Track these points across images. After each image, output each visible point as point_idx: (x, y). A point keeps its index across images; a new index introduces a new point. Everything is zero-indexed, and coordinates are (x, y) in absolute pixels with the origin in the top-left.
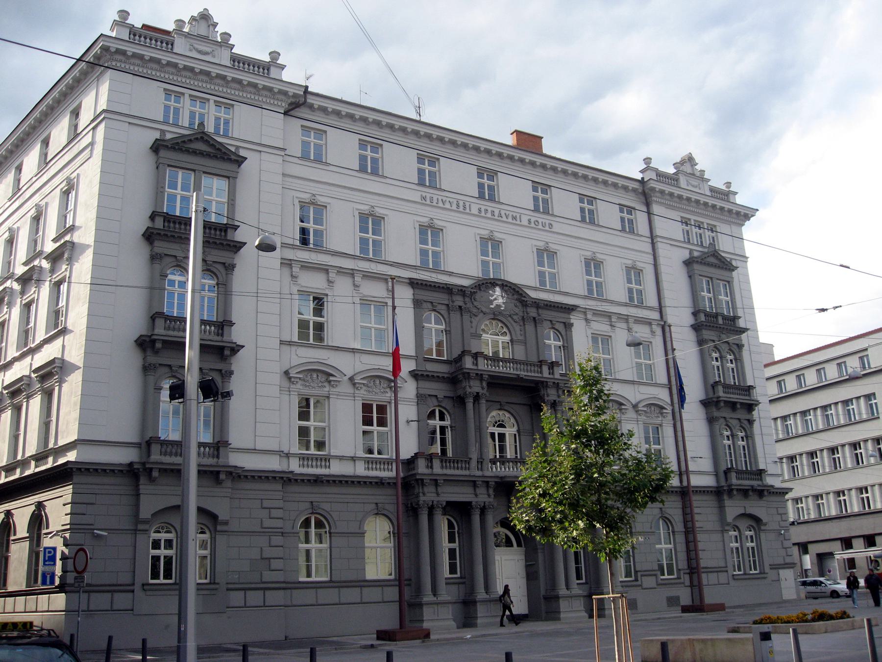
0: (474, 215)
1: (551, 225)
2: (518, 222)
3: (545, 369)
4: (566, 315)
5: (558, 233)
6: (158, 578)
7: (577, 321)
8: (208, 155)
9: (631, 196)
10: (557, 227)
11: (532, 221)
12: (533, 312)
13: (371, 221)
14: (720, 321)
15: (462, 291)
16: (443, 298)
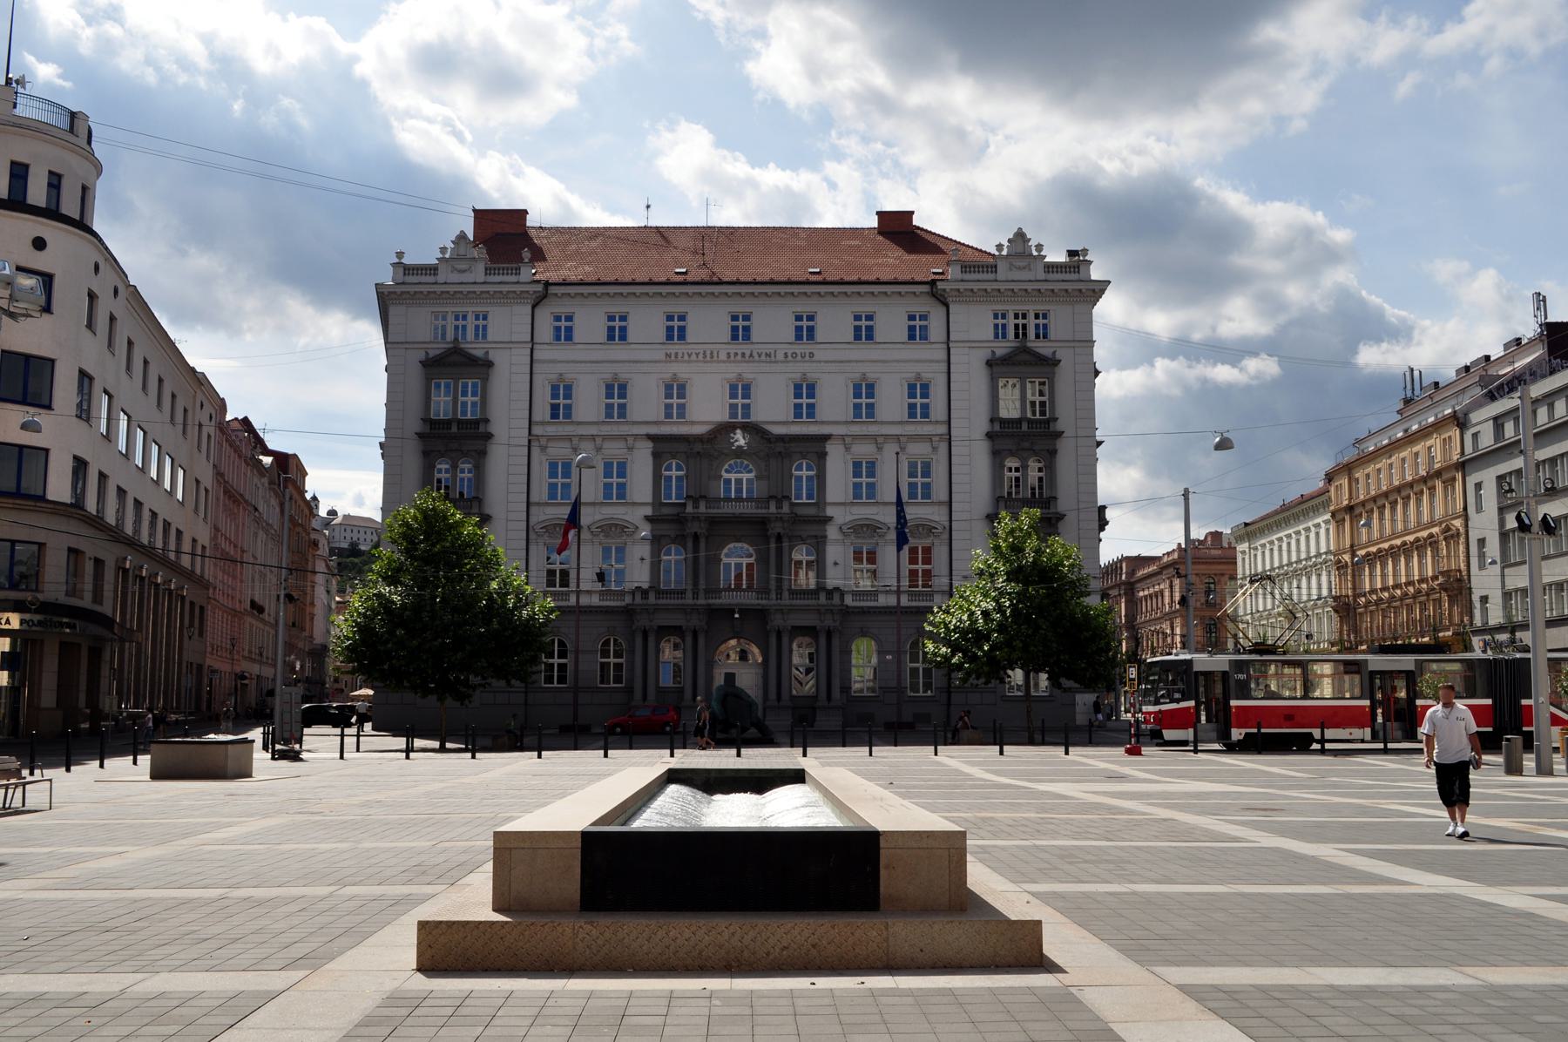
7: (834, 452)
10: (819, 355)
12: (780, 447)
13: (617, 389)
15: (699, 438)
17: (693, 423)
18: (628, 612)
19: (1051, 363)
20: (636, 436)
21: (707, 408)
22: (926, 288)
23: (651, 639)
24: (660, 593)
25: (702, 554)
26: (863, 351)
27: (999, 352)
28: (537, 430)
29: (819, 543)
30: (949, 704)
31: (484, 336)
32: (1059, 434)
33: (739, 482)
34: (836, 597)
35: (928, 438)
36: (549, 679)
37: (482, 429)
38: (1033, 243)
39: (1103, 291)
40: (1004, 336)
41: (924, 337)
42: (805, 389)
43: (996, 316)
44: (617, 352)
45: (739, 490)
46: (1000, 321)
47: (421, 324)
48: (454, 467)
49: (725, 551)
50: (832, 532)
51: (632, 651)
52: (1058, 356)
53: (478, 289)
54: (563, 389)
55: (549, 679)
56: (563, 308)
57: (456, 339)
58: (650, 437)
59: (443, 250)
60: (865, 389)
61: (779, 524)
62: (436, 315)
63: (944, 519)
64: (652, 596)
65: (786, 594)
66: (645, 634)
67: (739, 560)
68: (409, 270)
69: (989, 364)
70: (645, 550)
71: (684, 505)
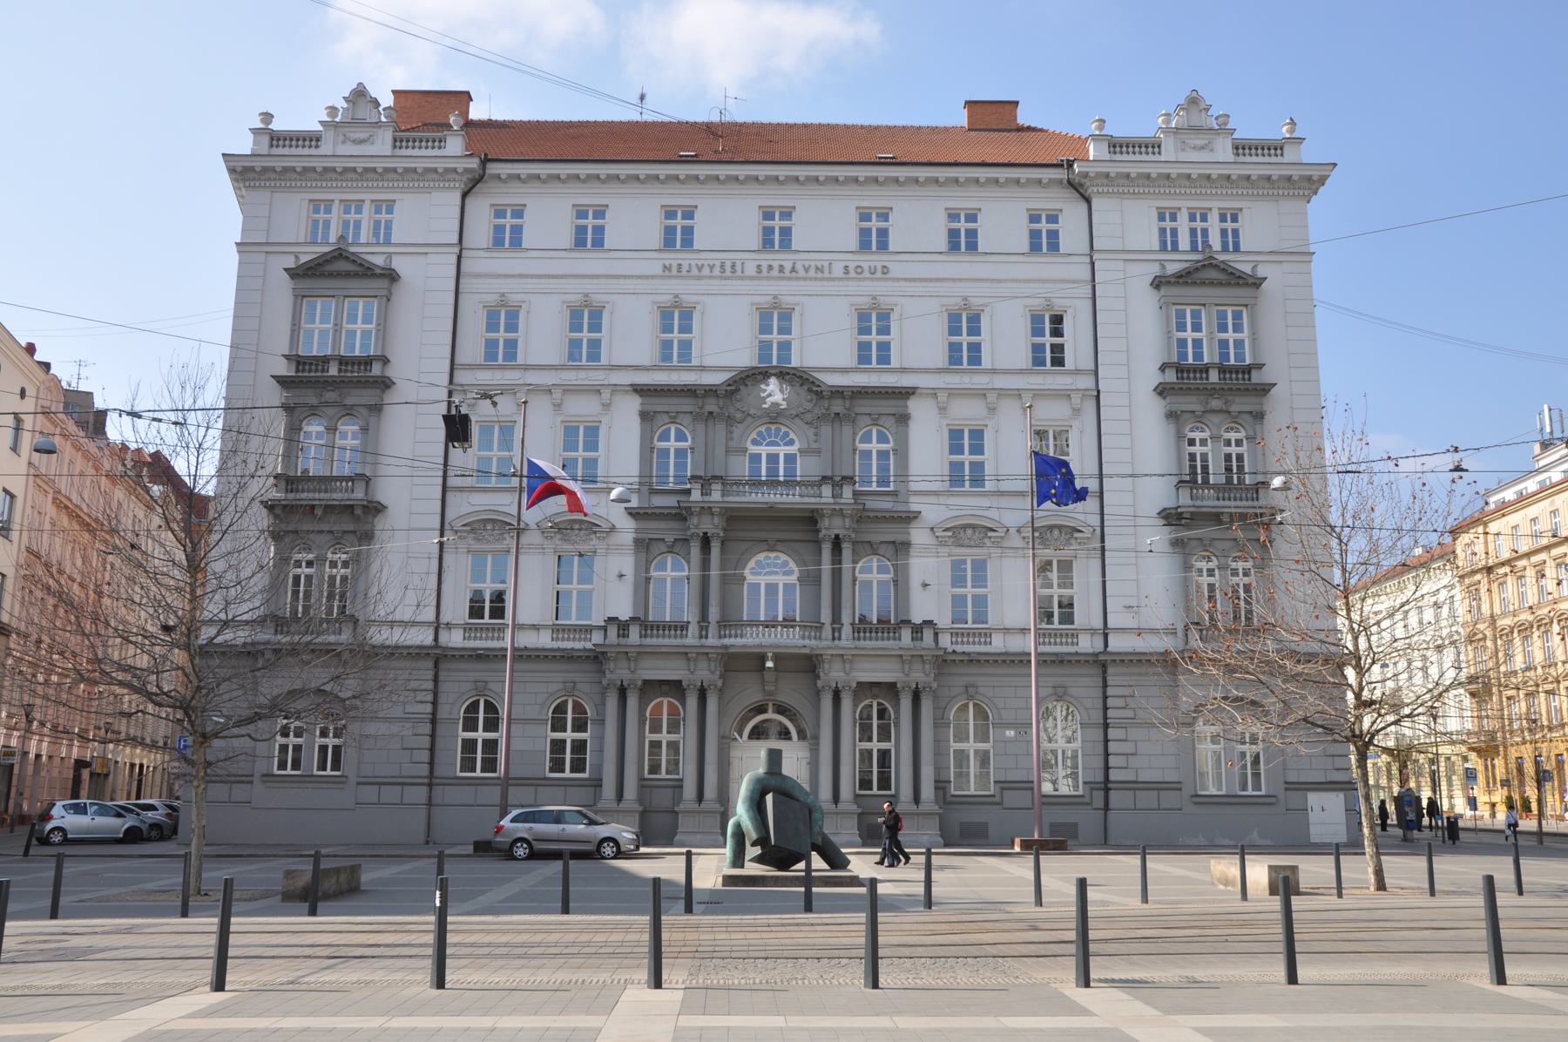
0: (752, 278)
1: (885, 270)
2: (826, 275)
3: (827, 491)
4: (900, 402)
5: (898, 280)
6: (324, 769)
7: (918, 409)
8: (356, 275)
9: (1057, 192)
10: (897, 270)
11: (851, 269)
12: (838, 407)
13: (586, 317)
14: (1214, 376)
15: (711, 391)
16: (687, 404)
17: (702, 368)
18: (596, 658)
19: (1256, 283)
20: (615, 389)
21: (724, 345)
22: (1060, 174)
23: (632, 702)
24: (647, 627)
25: (714, 572)
26: (962, 266)
27: (1172, 268)
28: (462, 377)
29: (902, 548)
30: (1106, 808)
31: (388, 234)
32: (1265, 389)
33: (773, 458)
34: (928, 635)
35: (1066, 395)
36: (469, 765)
37: (376, 369)
38: (1214, 112)
39: (1322, 181)
40: (1175, 248)
41: (1054, 246)
42: (873, 321)
43: (1162, 218)
44: (589, 263)
45: (773, 471)
46: (1168, 224)
47: (296, 224)
48: (332, 429)
49: (752, 564)
50: (919, 536)
51: (601, 722)
52: (1261, 272)
53: (379, 165)
54: (504, 315)
55: (469, 765)
56: (509, 196)
57: (342, 238)
58: (641, 390)
59: (332, 110)
60: (964, 323)
61: (837, 522)
62: (315, 205)
63: (1096, 521)
64: (634, 631)
65: (847, 631)
66: (623, 693)
67: (772, 579)
68: (277, 138)
69: (1158, 283)
70: (626, 562)
71: (688, 492)
